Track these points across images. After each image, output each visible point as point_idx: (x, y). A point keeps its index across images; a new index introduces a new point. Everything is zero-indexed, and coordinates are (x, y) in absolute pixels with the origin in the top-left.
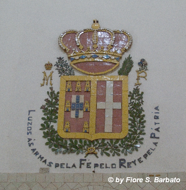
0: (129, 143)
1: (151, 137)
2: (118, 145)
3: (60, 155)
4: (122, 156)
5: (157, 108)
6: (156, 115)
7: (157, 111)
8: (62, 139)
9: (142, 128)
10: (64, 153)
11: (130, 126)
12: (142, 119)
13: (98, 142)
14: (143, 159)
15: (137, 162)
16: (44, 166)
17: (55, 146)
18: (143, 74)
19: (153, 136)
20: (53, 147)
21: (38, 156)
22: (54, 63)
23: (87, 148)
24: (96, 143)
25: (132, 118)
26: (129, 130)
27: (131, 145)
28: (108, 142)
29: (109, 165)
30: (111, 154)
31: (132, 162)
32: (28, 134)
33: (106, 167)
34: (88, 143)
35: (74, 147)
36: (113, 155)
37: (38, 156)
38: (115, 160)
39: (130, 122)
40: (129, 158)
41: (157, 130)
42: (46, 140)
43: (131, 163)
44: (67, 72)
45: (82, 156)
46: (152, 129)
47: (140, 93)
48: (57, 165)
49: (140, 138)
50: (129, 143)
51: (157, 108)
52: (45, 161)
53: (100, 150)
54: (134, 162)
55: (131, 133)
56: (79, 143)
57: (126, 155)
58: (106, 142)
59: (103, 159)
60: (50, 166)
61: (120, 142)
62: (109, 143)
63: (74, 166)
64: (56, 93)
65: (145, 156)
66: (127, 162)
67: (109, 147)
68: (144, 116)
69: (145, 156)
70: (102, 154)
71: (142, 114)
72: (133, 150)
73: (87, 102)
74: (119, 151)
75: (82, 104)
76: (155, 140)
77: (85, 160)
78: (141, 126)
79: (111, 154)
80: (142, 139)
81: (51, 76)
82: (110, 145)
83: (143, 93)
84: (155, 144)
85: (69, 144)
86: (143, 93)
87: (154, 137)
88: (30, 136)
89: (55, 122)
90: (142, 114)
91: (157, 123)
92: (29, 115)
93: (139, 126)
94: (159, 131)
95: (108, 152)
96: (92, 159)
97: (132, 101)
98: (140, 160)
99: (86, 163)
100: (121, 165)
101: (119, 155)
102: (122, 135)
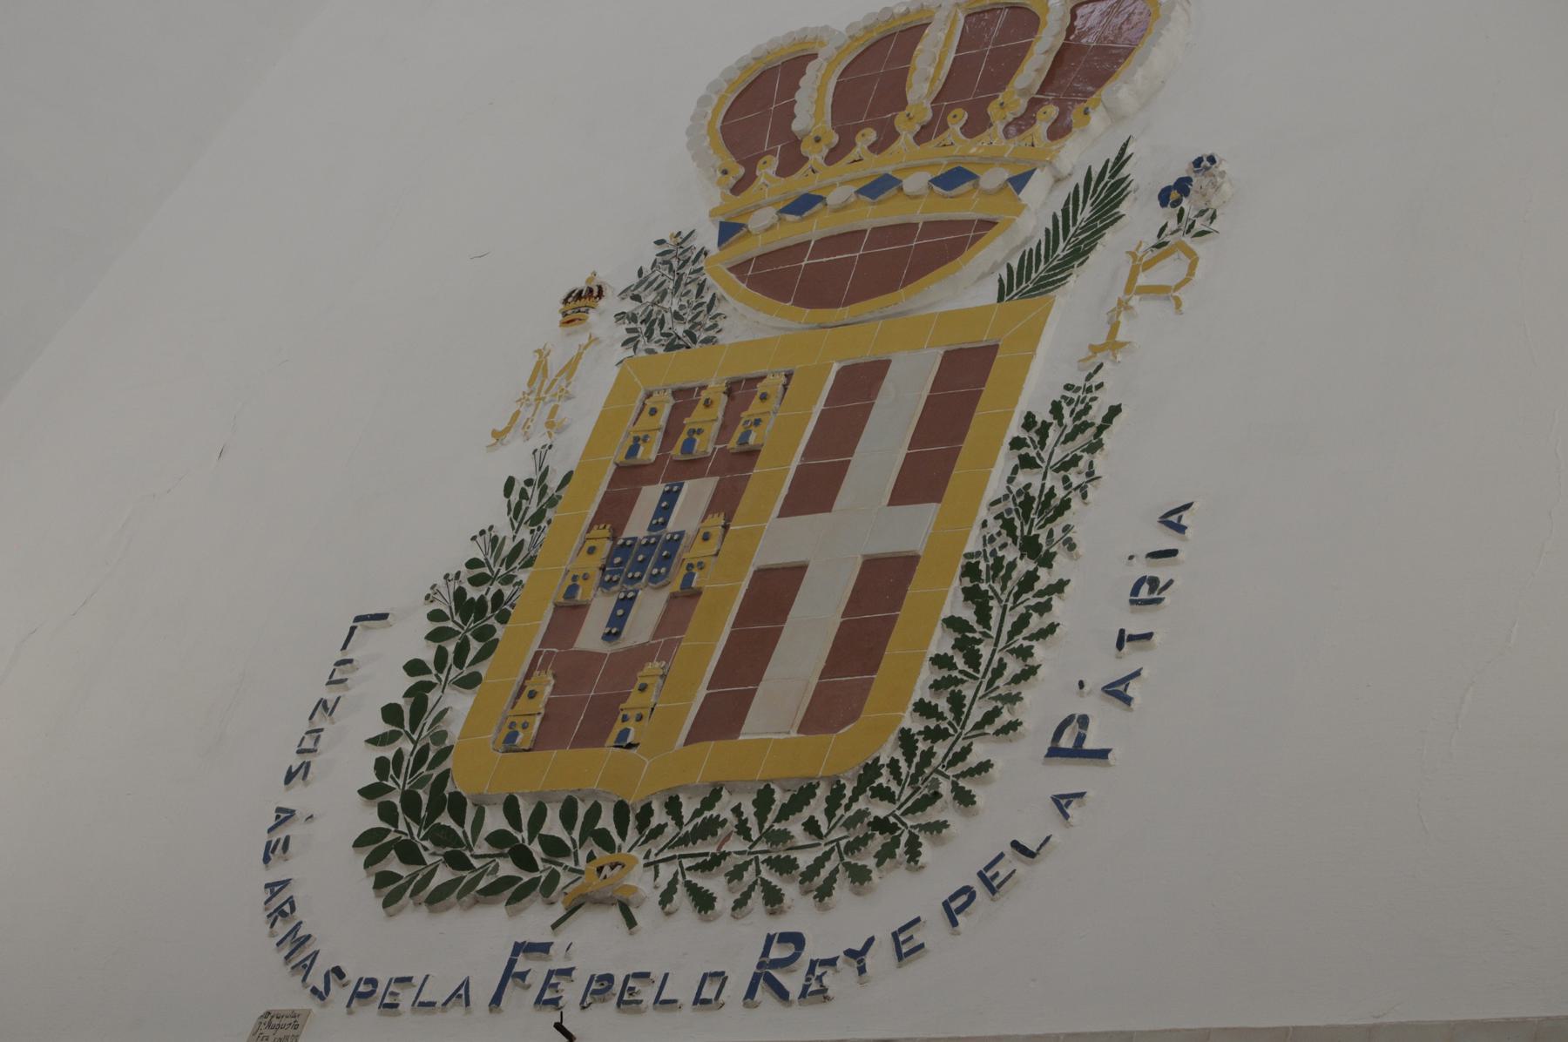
0: (880, 810)
1: (1055, 752)
2: (795, 827)
3: (413, 919)
4: (800, 913)
5: (1172, 520)
6: (1162, 571)
7: (1167, 540)
8: (457, 806)
9: (1016, 679)
10: (437, 899)
11: (927, 674)
12: (1044, 608)
13: (673, 806)
14: (933, 932)
15: (881, 957)
16: (290, 995)
17: (409, 853)
18: (1167, 271)
19: (1071, 746)
20: (393, 864)
21: (282, 928)
22: (618, 278)
23: (591, 857)
24: (659, 817)
25: (968, 614)
26: (923, 709)
27: (881, 825)
28: (737, 811)
29: (682, 989)
30: (724, 901)
31: (850, 953)
32: (290, 776)
33: (662, 1003)
34: (606, 822)
35: (527, 863)
36: (740, 904)
37: (282, 928)
38: (737, 941)
39: (942, 642)
40: (828, 927)
41: (1117, 691)
42: (370, 819)
43: (831, 962)
44: (680, 330)
45: (535, 921)
46: (1081, 685)
47: (1096, 415)
48: (364, 992)
49: (973, 760)
50: (880, 810)
51: (1172, 520)
52: (306, 967)
53: (667, 872)
54: (856, 955)
55: (915, 724)
56: (553, 826)
57: (824, 892)
58: (723, 809)
59: (676, 945)
60: (320, 995)
61: (816, 808)
62: (749, 811)
63: (462, 994)
64: (553, 482)
65: (956, 907)
66: (811, 952)
67: (736, 845)
68: (1059, 587)
69: (956, 907)
70: (666, 898)
71: (1045, 578)
72: (885, 854)
73: (720, 520)
74: (784, 866)
75: (674, 543)
76: (1070, 776)
77: (544, 948)
78: (1014, 667)
79: (724, 901)
80: (985, 767)
81: (570, 368)
82: (743, 830)
83: (1115, 411)
84: (1062, 803)
85: (497, 839)
86: (1115, 411)
87: (1079, 752)
88: (292, 798)
89: (470, 682)
90: (1045, 578)
91: (1132, 638)
92: (344, 647)
93: (999, 671)
94: (1127, 700)
95: (714, 883)
96: (594, 943)
97: (1022, 478)
98: (905, 947)
99: (536, 969)
100: (765, 978)
101: (773, 898)
102: (839, 755)
